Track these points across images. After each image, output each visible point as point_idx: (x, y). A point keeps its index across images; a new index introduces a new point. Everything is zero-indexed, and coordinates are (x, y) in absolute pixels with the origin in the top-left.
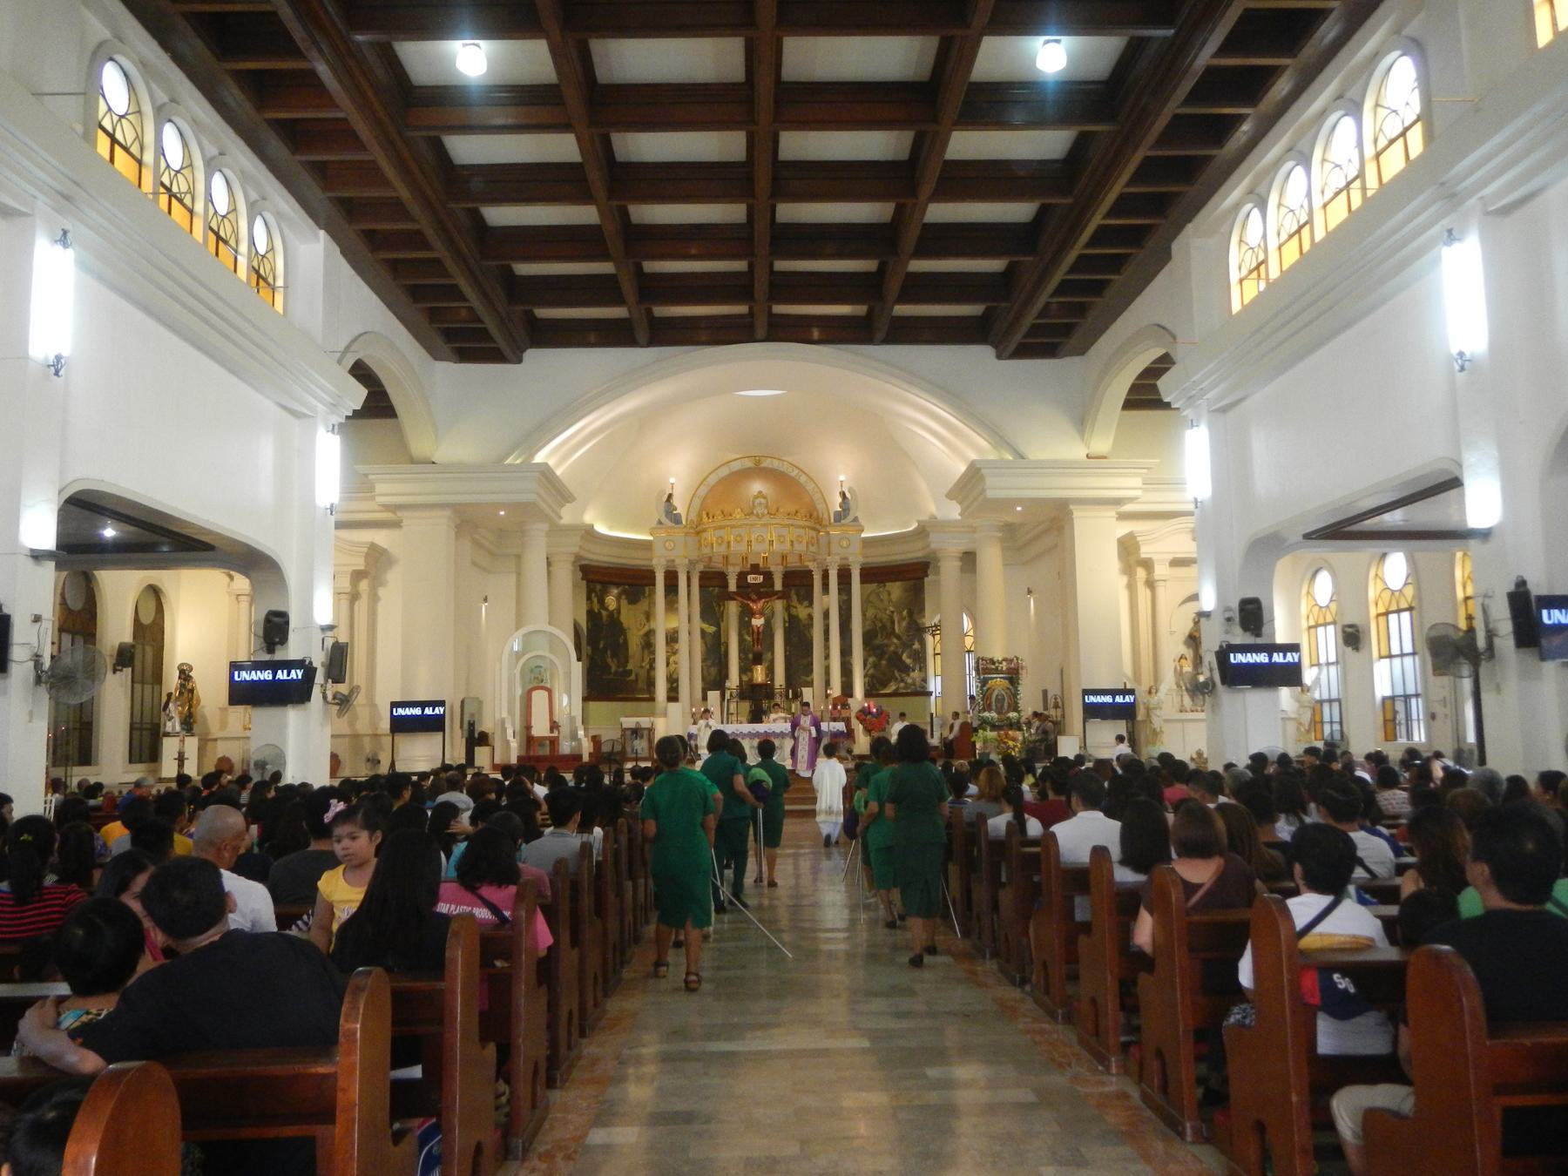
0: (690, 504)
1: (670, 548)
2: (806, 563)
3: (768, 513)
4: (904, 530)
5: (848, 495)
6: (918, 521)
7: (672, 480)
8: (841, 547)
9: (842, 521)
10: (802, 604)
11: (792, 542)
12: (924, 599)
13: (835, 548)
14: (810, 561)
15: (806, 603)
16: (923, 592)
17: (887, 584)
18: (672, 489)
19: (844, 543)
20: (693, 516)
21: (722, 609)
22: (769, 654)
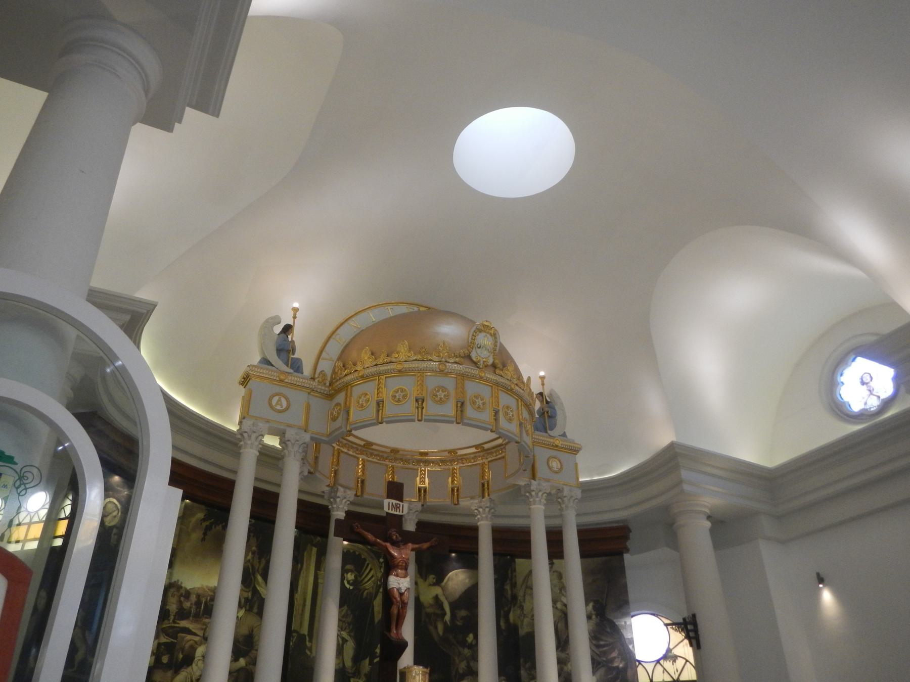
0: (333, 333)
1: (278, 407)
2: (465, 503)
3: (494, 366)
4: (596, 478)
5: (548, 400)
6: (672, 446)
7: (296, 305)
8: (550, 468)
9: (549, 432)
10: (425, 580)
11: (521, 424)
12: (625, 586)
13: (542, 470)
14: (472, 498)
15: (432, 578)
16: (625, 577)
17: (555, 561)
18: (295, 317)
19: (555, 465)
20: (326, 366)
21: (299, 565)
22: (367, 661)
